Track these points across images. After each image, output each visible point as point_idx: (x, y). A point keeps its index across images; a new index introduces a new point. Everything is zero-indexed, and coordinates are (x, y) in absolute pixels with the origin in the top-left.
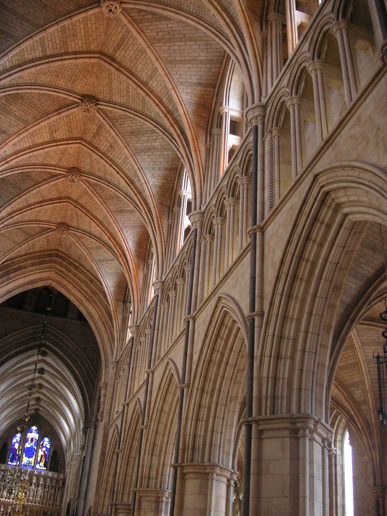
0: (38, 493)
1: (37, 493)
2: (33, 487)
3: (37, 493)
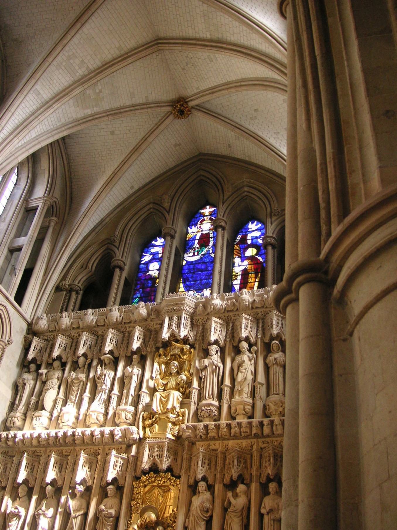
0: (240, 377)
1: (233, 380)
2: (216, 358)
3: (233, 380)
